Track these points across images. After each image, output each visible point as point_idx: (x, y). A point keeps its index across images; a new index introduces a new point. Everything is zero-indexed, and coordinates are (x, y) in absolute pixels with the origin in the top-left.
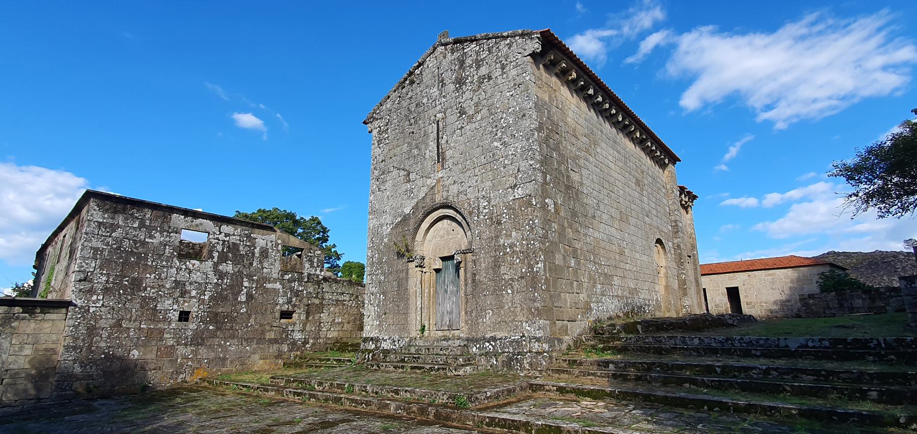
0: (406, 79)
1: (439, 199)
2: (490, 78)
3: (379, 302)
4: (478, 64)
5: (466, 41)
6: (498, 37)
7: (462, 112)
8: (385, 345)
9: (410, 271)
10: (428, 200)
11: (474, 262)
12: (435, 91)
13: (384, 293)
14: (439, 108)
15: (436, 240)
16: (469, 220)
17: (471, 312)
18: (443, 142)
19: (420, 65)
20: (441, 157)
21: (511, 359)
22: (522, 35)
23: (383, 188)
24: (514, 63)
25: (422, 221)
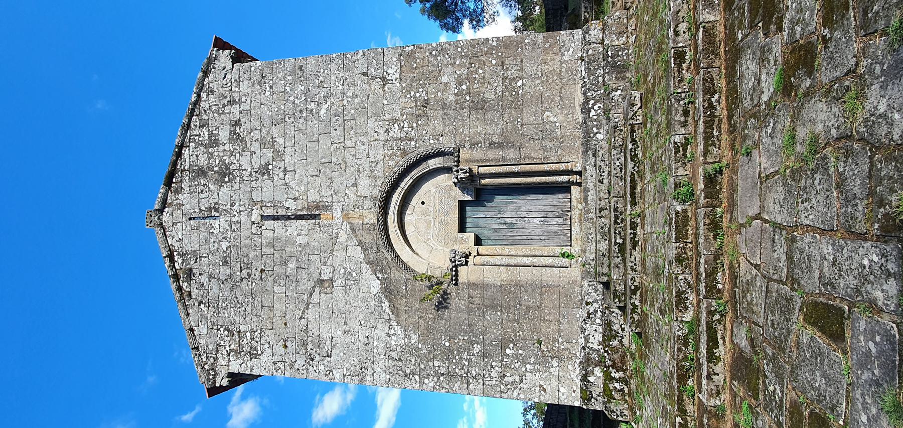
0: (180, 289)
1: (371, 217)
2: (237, 123)
3: (517, 357)
4: (214, 142)
5: (175, 164)
6: (193, 110)
7: (265, 170)
8: (596, 340)
9: (473, 279)
10: (368, 239)
11: (473, 145)
12: (220, 224)
13: (504, 347)
14: (244, 217)
15: (430, 235)
16: (411, 158)
17: (545, 149)
18: (293, 207)
19: (171, 257)
20: (311, 215)
21: (614, 66)
22: (206, 73)
23: (327, 347)
24: (234, 85)
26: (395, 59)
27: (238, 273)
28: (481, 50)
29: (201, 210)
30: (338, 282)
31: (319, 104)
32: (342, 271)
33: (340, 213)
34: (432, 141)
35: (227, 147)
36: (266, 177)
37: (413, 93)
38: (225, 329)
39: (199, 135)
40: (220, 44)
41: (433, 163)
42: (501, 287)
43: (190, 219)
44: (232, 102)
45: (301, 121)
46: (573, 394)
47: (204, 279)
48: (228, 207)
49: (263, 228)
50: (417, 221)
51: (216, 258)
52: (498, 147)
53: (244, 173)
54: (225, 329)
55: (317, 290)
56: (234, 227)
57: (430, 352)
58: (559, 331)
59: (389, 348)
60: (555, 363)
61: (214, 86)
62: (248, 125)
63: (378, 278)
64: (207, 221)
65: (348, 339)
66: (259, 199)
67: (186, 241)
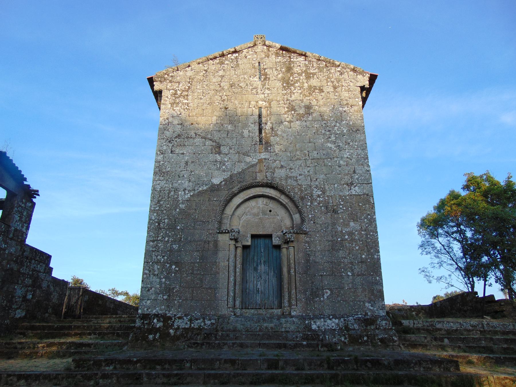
1: (260, 178)
4: (309, 76)
5: (294, 52)
12: (256, 81)
13: (177, 264)
19: (235, 52)
25: (235, 195)
26: (364, 191)
27: (225, 94)
28: (371, 248)
29: (265, 69)
30: (218, 158)
31: (334, 143)
32: (226, 160)
33: (264, 157)
34: (310, 216)
35: (306, 85)
36: (286, 109)
37: (342, 203)
38: (189, 87)
39: (313, 66)
40: (373, 79)
41: (297, 217)
42: (215, 262)
43: (259, 63)
44: (335, 88)
45: (323, 131)
46: (145, 309)
47: (221, 73)
48: (267, 86)
49: (254, 109)
50: (259, 207)
51: (235, 78)
52: (307, 260)
53: (289, 96)
54: (189, 87)
55: (214, 144)
56: (255, 90)
57: (174, 216)
58: (186, 299)
59: (176, 190)
60: (165, 297)
61: (345, 76)
62: (320, 97)
63: (220, 183)
64: (258, 73)
65: (183, 164)
66: (272, 105)
67: (245, 60)
